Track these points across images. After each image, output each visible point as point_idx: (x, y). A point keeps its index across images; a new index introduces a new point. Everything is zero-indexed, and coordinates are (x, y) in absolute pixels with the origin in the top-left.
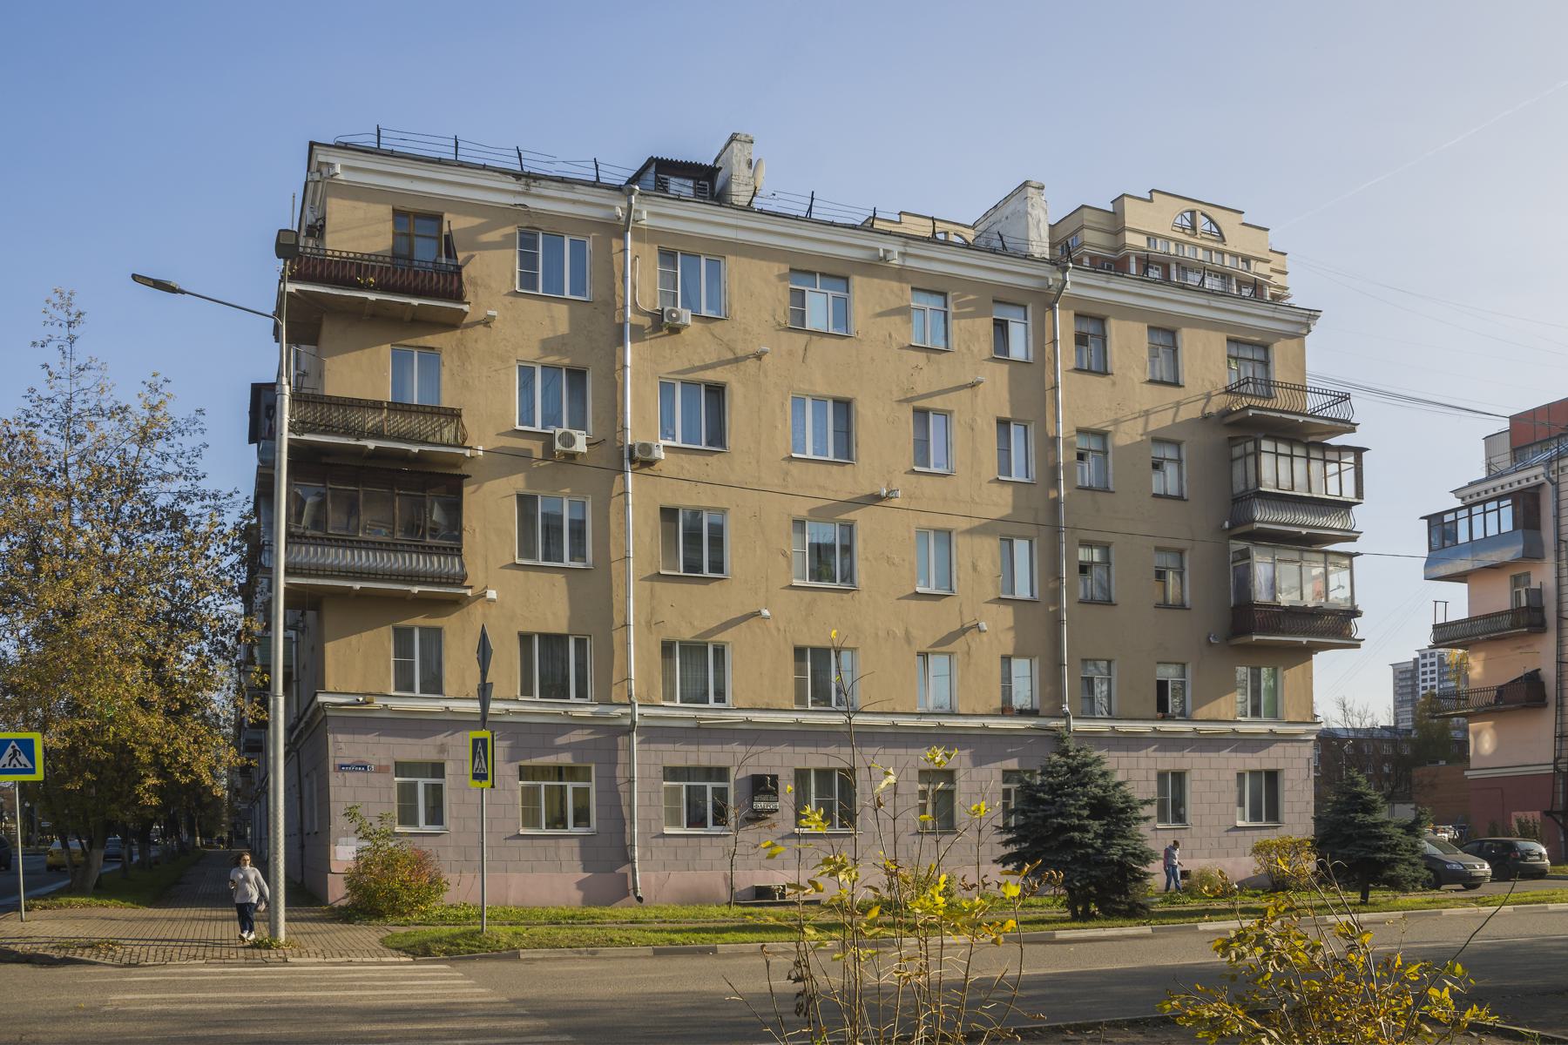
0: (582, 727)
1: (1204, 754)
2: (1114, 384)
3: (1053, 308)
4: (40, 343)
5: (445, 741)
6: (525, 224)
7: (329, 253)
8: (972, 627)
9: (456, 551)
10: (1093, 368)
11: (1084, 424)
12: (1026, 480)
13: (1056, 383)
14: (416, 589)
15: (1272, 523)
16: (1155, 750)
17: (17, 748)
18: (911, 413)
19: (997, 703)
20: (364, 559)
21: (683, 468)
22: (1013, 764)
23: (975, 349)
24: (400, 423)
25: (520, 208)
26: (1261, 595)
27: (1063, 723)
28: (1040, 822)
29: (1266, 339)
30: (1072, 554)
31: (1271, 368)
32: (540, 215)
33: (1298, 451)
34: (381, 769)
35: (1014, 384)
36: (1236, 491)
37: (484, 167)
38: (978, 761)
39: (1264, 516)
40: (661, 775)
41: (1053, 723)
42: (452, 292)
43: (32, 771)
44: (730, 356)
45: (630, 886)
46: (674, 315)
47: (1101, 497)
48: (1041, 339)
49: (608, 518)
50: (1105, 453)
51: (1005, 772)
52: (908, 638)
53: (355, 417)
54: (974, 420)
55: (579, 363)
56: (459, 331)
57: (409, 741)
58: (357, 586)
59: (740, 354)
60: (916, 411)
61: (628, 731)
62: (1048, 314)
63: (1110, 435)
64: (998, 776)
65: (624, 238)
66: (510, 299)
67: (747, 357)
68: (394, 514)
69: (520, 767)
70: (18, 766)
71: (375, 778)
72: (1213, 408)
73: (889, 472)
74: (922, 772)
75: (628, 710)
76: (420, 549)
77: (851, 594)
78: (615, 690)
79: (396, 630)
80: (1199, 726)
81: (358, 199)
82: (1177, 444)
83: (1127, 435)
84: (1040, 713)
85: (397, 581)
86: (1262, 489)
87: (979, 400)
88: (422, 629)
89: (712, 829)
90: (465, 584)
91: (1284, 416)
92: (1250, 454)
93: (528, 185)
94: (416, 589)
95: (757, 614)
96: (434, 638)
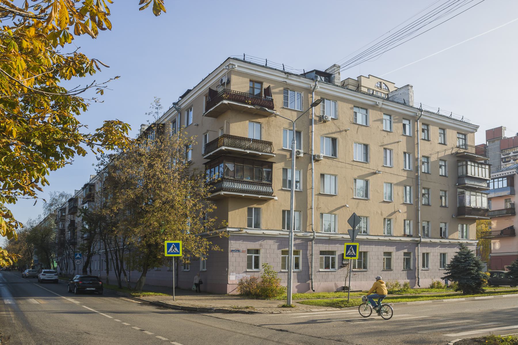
0: (299, 239)
1: (451, 249)
2: (431, 144)
3: (417, 121)
4: (148, 113)
5: (261, 243)
6: (286, 87)
7: (232, 91)
8: (397, 211)
9: (270, 185)
10: (426, 139)
11: (424, 155)
12: (409, 170)
13: (418, 143)
14: (260, 196)
15: (469, 184)
16: (439, 247)
17: (174, 246)
18: (383, 149)
19: (403, 233)
20: (245, 187)
21: (326, 162)
22: (406, 251)
23: (399, 132)
24: (255, 145)
25: (285, 82)
26: (467, 205)
27: (419, 239)
28: (463, 268)
29: (466, 133)
30: (421, 191)
31: (466, 141)
32: (290, 85)
33: (476, 165)
34: (243, 252)
35: (408, 143)
36: (459, 175)
37: (276, 69)
38: (398, 250)
39: (468, 183)
40: (319, 253)
41: (417, 239)
42: (271, 107)
43: (179, 253)
44: (339, 130)
45: (311, 287)
46: (326, 118)
47: (427, 174)
48: (414, 130)
49: (307, 176)
50: (428, 163)
51: (404, 253)
52: (382, 214)
53: (243, 143)
54: (398, 152)
55: (299, 130)
56: (267, 118)
57: (252, 243)
58: (244, 195)
59: (341, 130)
60: (384, 149)
61: (311, 240)
62: (416, 123)
63: (429, 158)
64: (403, 254)
65: (312, 94)
66: (282, 109)
67: (343, 131)
68: (253, 173)
69: (282, 251)
70: (175, 252)
71: (241, 254)
72: (454, 152)
73: (378, 166)
74: (384, 253)
75: (313, 234)
76: (259, 184)
77: (368, 201)
78: (308, 228)
79: (248, 208)
80: (450, 241)
81: (240, 76)
82: (445, 161)
83: (433, 159)
84: (413, 236)
85: (254, 194)
86: (468, 175)
87: (399, 146)
88: (255, 208)
89: (331, 269)
90: (272, 195)
91: (473, 155)
92: (464, 165)
93: (288, 76)
94: (260, 196)
95: (345, 206)
96: (258, 210)
